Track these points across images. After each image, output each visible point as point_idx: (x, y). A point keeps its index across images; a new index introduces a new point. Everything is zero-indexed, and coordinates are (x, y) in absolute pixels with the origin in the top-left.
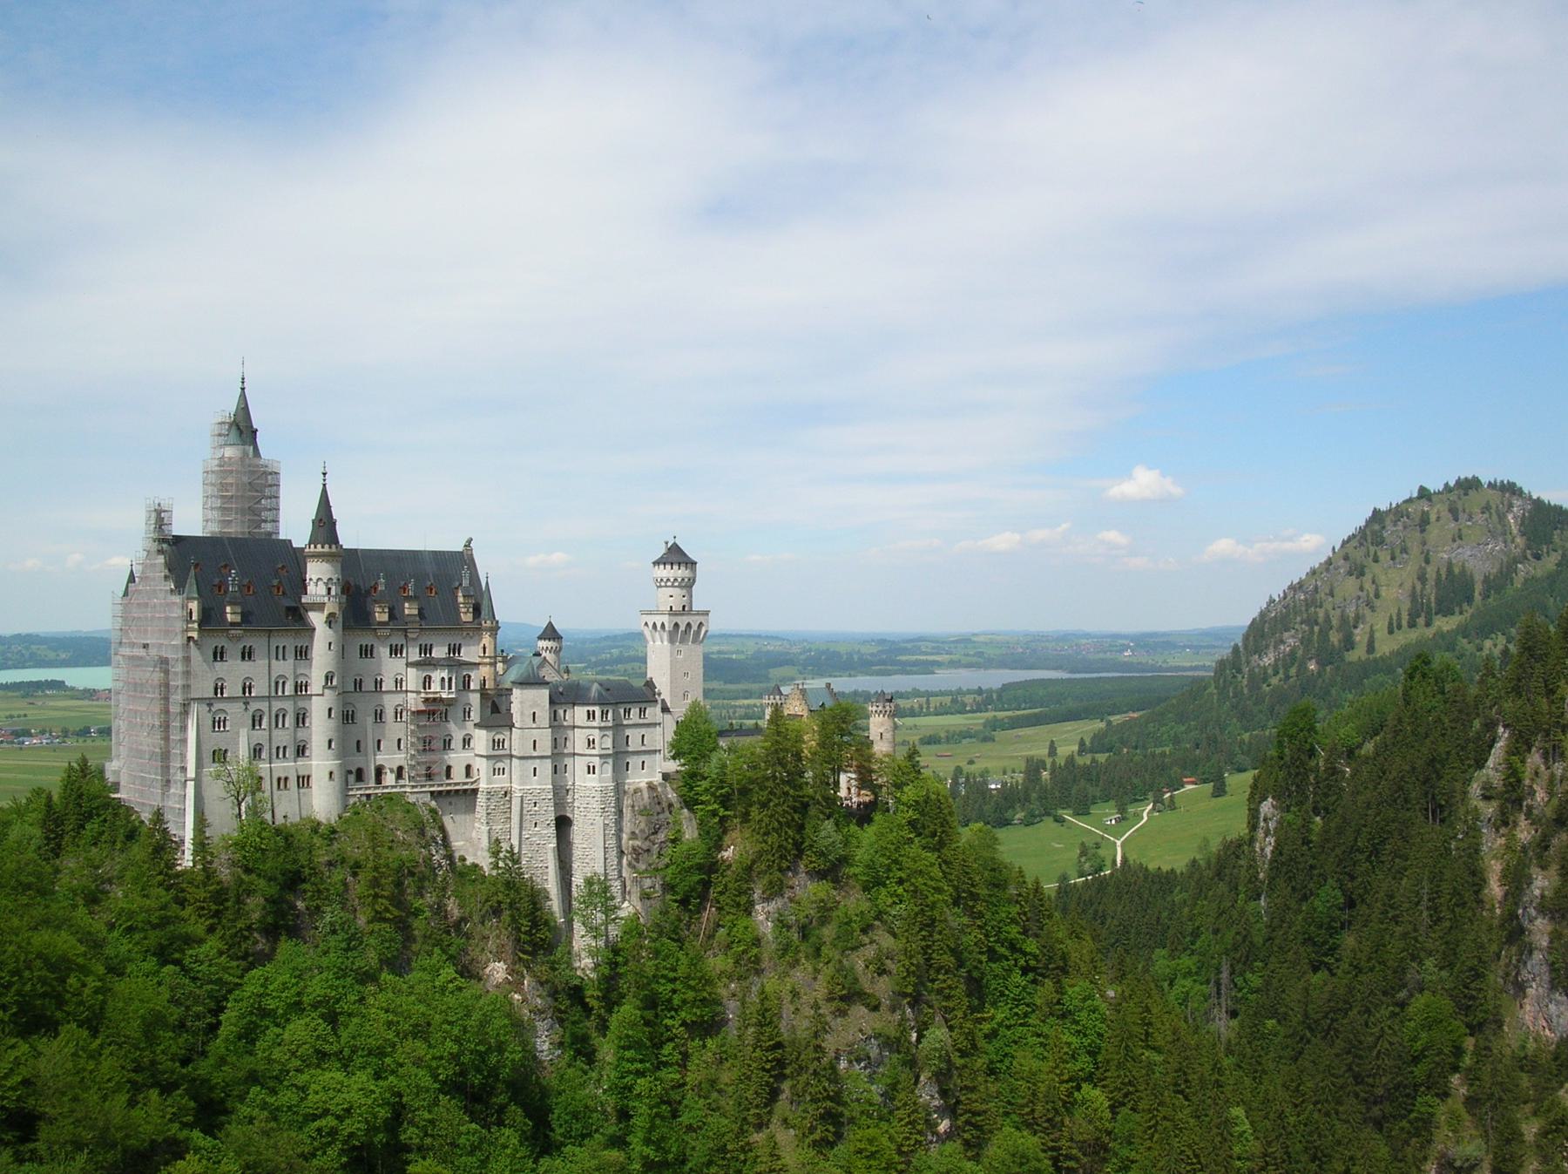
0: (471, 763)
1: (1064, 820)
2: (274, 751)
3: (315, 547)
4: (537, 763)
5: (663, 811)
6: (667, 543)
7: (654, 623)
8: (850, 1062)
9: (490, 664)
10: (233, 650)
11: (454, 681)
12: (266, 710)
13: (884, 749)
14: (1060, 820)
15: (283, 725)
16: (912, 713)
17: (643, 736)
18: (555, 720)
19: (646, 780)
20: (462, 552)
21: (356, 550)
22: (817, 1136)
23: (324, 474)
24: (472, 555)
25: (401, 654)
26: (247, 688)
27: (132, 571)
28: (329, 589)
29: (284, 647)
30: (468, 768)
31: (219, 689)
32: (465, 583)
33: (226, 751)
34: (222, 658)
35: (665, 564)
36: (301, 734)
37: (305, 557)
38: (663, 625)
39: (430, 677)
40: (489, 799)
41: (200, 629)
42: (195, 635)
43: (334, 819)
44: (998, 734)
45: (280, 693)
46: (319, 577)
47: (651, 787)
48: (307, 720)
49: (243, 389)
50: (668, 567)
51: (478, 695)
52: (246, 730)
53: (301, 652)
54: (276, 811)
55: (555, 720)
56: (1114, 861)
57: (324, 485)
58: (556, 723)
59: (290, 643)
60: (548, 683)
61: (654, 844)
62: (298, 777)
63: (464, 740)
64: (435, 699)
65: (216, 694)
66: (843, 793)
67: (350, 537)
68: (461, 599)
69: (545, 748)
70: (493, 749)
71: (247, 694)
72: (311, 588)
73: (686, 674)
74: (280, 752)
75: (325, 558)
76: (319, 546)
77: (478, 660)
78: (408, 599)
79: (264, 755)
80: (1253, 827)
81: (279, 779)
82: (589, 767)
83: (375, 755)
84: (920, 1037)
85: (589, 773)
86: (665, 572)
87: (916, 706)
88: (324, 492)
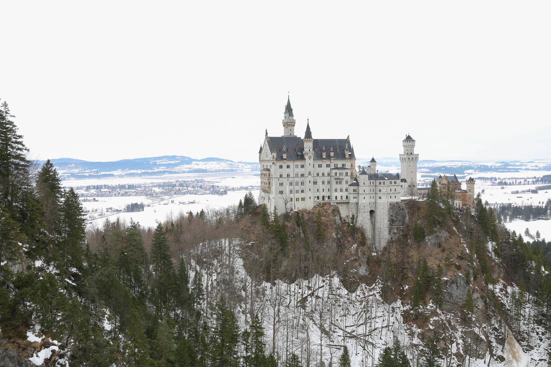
2: (295, 191)
4: (365, 195)
5: (401, 210)
6: (406, 135)
10: (285, 166)
12: (293, 181)
16: (510, 184)
17: (395, 189)
18: (370, 184)
23: (308, 120)
26: (288, 176)
31: (281, 176)
32: (347, 147)
36: (303, 187)
37: (303, 142)
38: (405, 158)
41: (276, 160)
42: (275, 162)
44: (539, 191)
46: (308, 146)
47: (397, 203)
49: (289, 99)
50: (407, 142)
51: (349, 177)
54: (296, 206)
55: (370, 184)
59: (299, 163)
64: (338, 178)
67: (315, 136)
69: (367, 191)
73: (411, 172)
74: (297, 192)
78: (331, 152)
81: (297, 198)
86: (406, 144)
87: (512, 182)
88: (308, 125)
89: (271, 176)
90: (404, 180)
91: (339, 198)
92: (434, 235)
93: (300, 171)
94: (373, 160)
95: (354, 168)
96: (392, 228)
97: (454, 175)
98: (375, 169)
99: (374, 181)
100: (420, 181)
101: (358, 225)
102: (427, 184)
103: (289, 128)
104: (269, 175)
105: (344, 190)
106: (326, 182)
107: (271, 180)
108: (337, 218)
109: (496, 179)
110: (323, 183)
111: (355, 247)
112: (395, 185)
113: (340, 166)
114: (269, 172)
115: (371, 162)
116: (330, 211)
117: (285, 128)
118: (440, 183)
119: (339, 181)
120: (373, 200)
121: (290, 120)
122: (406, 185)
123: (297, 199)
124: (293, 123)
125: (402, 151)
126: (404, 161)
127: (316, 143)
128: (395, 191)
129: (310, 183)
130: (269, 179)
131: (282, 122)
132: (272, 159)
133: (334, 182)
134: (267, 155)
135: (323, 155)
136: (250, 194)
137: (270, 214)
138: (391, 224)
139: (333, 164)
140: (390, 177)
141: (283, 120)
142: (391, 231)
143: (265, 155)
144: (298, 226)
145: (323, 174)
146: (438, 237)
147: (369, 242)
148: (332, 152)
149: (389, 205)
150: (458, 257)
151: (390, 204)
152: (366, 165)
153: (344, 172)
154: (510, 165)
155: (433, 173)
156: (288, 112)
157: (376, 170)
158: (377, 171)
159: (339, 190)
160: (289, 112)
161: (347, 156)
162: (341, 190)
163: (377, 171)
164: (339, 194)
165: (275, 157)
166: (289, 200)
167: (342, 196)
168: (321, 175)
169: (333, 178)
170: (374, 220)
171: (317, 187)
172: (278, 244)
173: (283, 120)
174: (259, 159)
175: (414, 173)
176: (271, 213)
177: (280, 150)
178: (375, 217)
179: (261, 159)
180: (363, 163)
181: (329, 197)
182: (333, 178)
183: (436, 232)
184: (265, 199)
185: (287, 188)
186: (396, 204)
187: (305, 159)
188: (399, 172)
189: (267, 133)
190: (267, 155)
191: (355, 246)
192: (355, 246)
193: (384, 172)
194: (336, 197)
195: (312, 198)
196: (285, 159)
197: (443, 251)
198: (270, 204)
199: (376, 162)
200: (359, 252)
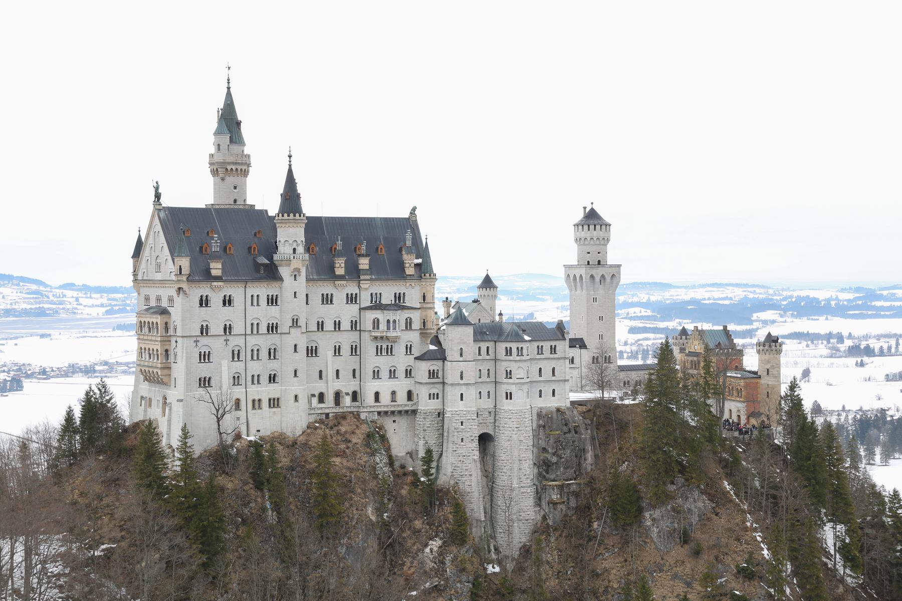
0: (412, 388)
2: (249, 379)
3: (283, 216)
4: (463, 390)
5: (569, 431)
6: (585, 208)
10: (216, 299)
11: (397, 322)
12: (243, 345)
13: (770, 383)
15: (258, 358)
16: (882, 353)
17: (554, 369)
18: (480, 354)
19: (556, 405)
20: (409, 219)
21: (321, 218)
23: (290, 156)
24: (416, 220)
25: (356, 301)
26: (227, 329)
27: (140, 237)
28: (294, 250)
29: (258, 296)
30: (410, 395)
31: (204, 331)
32: (409, 243)
33: (210, 378)
34: (207, 305)
35: (583, 226)
36: (273, 365)
37: (275, 224)
38: (581, 276)
39: (378, 320)
40: (424, 418)
42: (185, 286)
43: (299, 432)
45: (255, 332)
47: (558, 410)
48: (277, 353)
50: (586, 227)
52: (226, 361)
53: (272, 299)
54: (251, 426)
55: (480, 354)
57: (290, 166)
58: (480, 358)
59: (263, 290)
60: (471, 324)
61: (561, 458)
62: (270, 400)
63: (407, 370)
64: (382, 338)
65: (202, 333)
67: (311, 207)
68: (405, 257)
69: (471, 375)
70: (429, 378)
71: (228, 333)
72: (281, 249)
73: (601, 318)
75: (291, 225)
76: (286, 215)
77: (418, 306)
78: (359, 255)
79: (242, 381)
81: (254, 401)
82: (507, 393)
83: (333, 382)
85: (507, 398)
86: (585, 233)
87: (885, 346)
88: (290, 172)
89: (171, 332)
90: (578, 343)
91: (385, 399)
92: (669, 507)
93: (265, 314)
94: (487, 283)
96: (544, 488)
97: (721, 328)
98: (493, 309)
99: (491, 345)
100: (626, 344)
101: (443, 480)
102: (645, 353)
103: (231, 180)
104: (167, 328)
105: (401, 373)
106: (346, 350)
107: (173, 344)
108: (380, 460)
109: (840, 338)
110: (337, 351)
111: (435, 549)
112: (552, 356)
113: (388, 299)
114: (164, 318)
115: (481, 287)
116: (357, 439)
117: (218, 179)
118: (682, 350)
119: (384, 346)
120: (487, 404)
121: (232, 155)
122: (583, 357)
123: (256, 404)
124: (242, 164)
125: (571, 254)
126: (578, 284)
127: (315, 226)
128: (554, 374)
129: (295, 351)
130: (166, 340)
131: (207, 160)
132: (174, 278)
133: (369, 348)
134: (159, 266)
135: (337, 265)
136: (103, 389)
137: (168, 451)
138: (541, 476)
139: (367, 290)
140: (538, 332)
141: (212, 156)
142: (543, 496)
143: (154, 263)
144: (259, 486)
145: (337, 325)
146: (679, 512)
147: (476, 532)
148: (363, 255)
149: (535, 417)
150: (739, 572)
151: (539, 415)
152: (467, 296)
153: (401, 317)
154: (880, 298)
155: (662, 320)
156: (228, 132)
157: (498, 312)
158: (501, 314)
159: (385, 374)
160: (230, 131)
161: (410, 271)
162: (392, 374)
163: (501, 314)
164: (385, 386)
165: (186, 270)
166: (229, 405)
167: (394, 393)
168: (329, 326)
169: (366, 337)
170: (490, 462)
171: (317, 363)
172: (194, 546)
173: (212, 156)
174: (132, 278)
175: (606, 319)
176: (171, 447)
177: (201, 248)
178: (494, 456)
179: (140, 277)
180: (459, 291)
181: (355, 396)
182: (366, 337)
183: (673, 498)
184: (150, 405)
185: (225, 369)
186: (555, 416)
187: (279, 279)
188: (565, 317)
189: (158, 196)
190: (159, 266)
191: (435, 544)
192: (435, 544)
193: (519, 318)
194: (377, 395)
195: (303, 400)
196: (218, 278)
197: (697, 553)
198: (169, 421)
199: (495, 287)
200: (448, 563)
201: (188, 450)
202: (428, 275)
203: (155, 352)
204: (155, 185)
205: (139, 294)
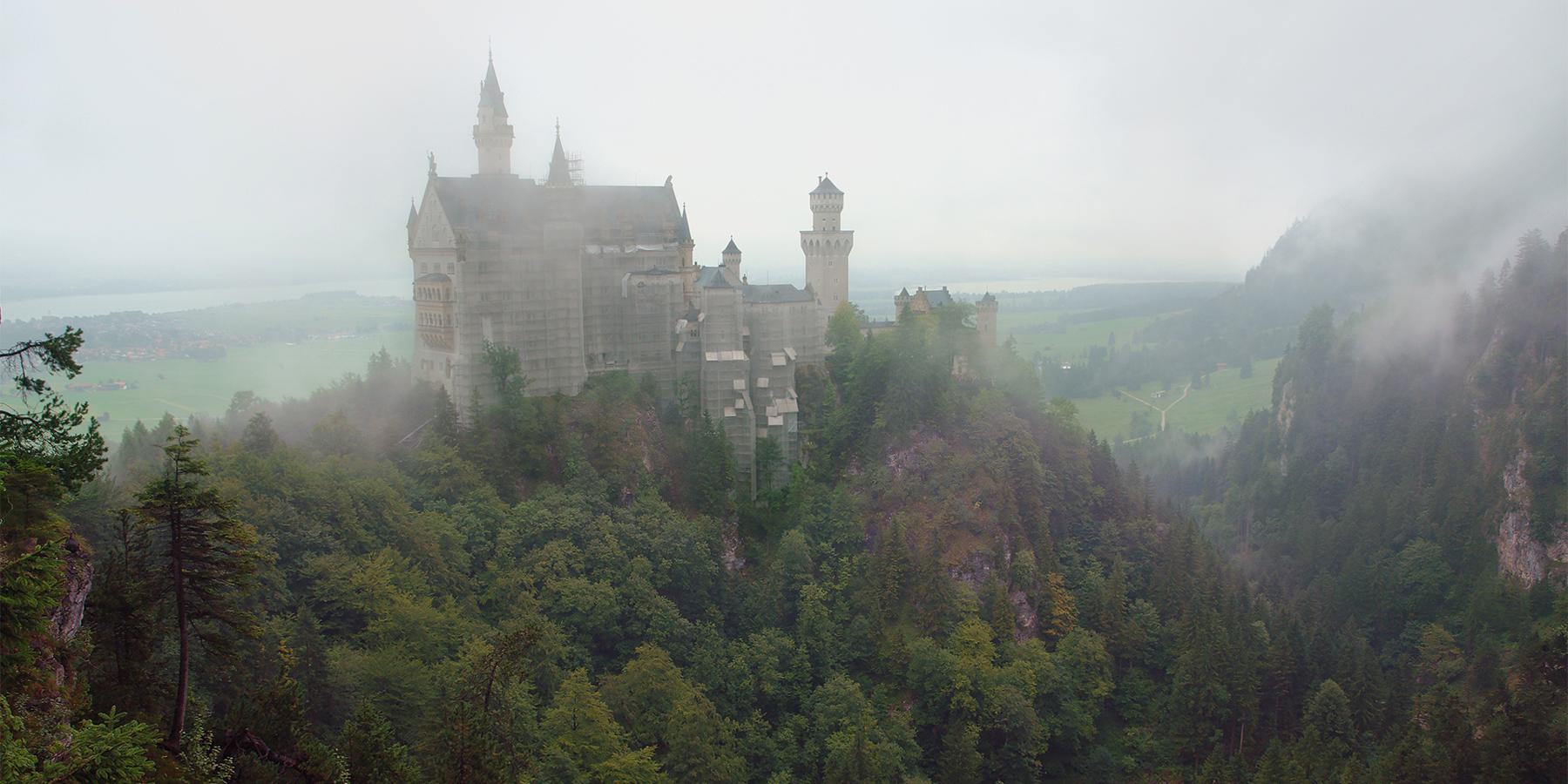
1: (1120, 394)
6: (820, 178)
7: (811, 241)
8: (960, 574)
9: (690, 273)
14: (1118, 395)
22: (935, 629)
23: (558, 127)
27: (413, 205)
35: (819, 194)
38: (818, 242)
49: (491, 61)
50: (822, 197)
56: (1160, 427)
57: (558, 136)
66: (955, 372)
77: (678, 271)
80: (1276, 403)
84: (1013, 557)
88: (558, 142)
94: (732, 250)
95: (691, 270)
97: (942, 289)
98: (737, 272)
104: (448, 295)
125: (807, 222)
158: (745, 278)
163: (745, 278)
179: (416, 246)
189: (433, 166)
201: (479, 409)
202: (687, 241)
203: (437, 317)
204: (430, 156)
205: (414, 261)
